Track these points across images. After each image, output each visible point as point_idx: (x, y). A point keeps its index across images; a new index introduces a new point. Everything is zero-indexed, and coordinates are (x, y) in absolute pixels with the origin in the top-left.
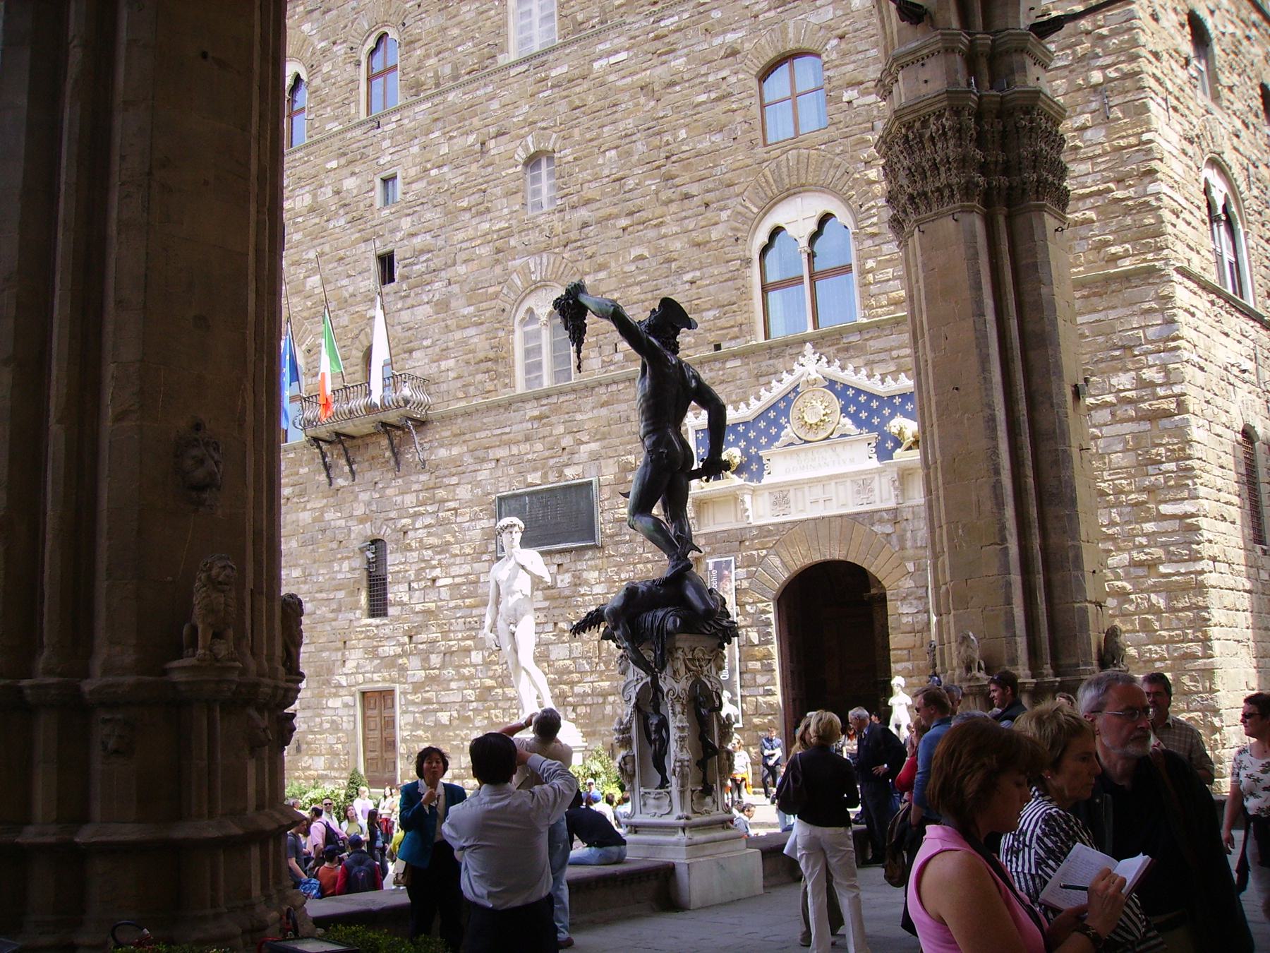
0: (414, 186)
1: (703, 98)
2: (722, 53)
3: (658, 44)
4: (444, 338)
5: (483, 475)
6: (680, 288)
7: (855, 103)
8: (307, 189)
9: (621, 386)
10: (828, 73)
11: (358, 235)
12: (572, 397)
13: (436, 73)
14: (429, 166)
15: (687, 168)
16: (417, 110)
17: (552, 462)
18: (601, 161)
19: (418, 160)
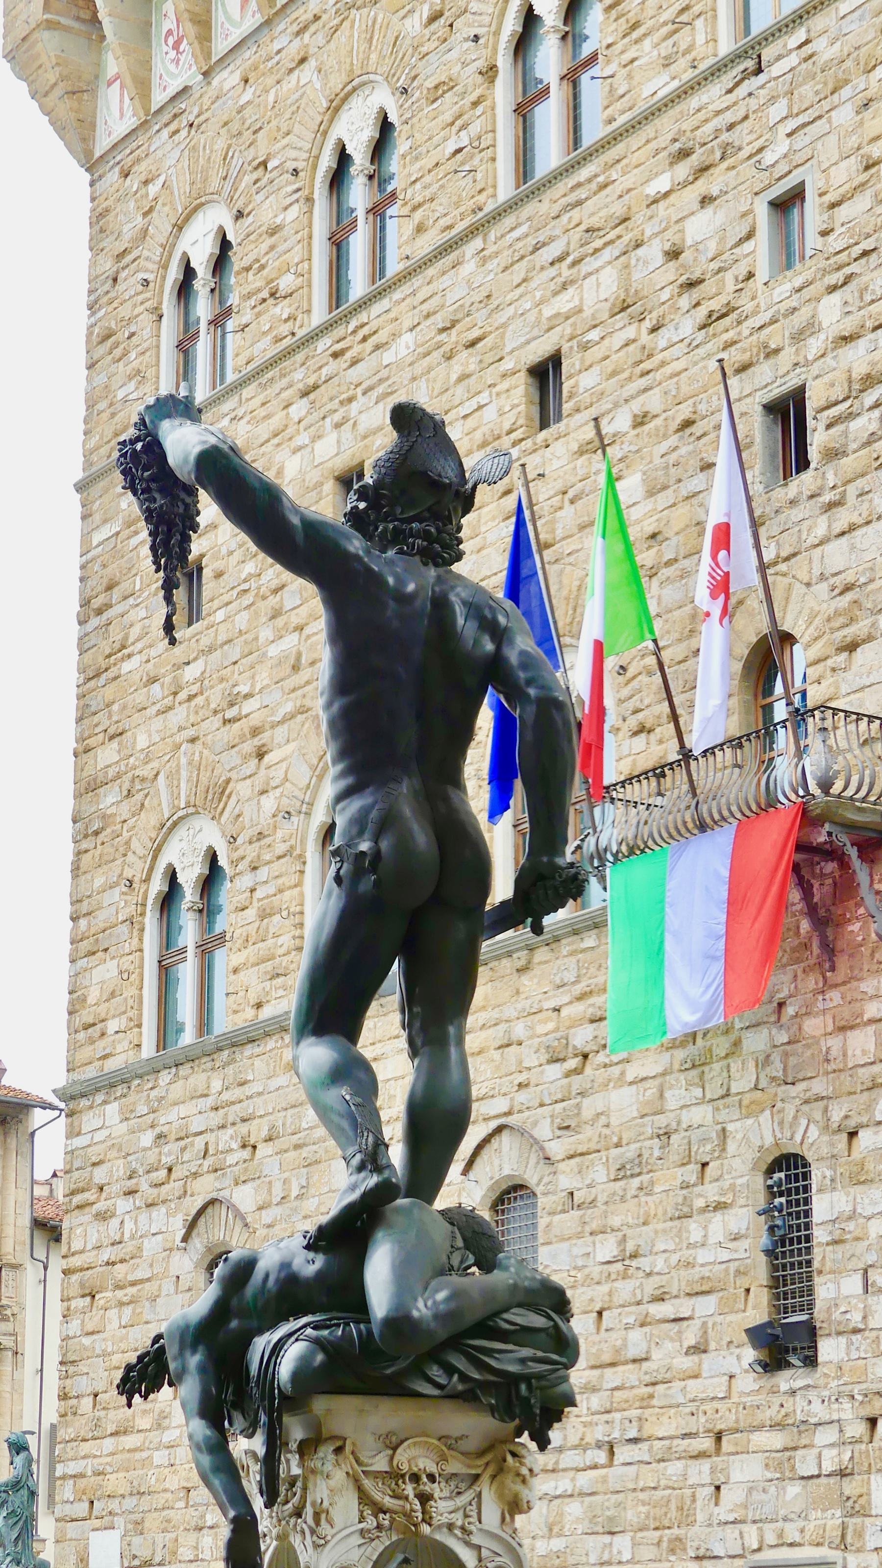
0: (843, 212)
8: (607, 254)
19: (853, 141)
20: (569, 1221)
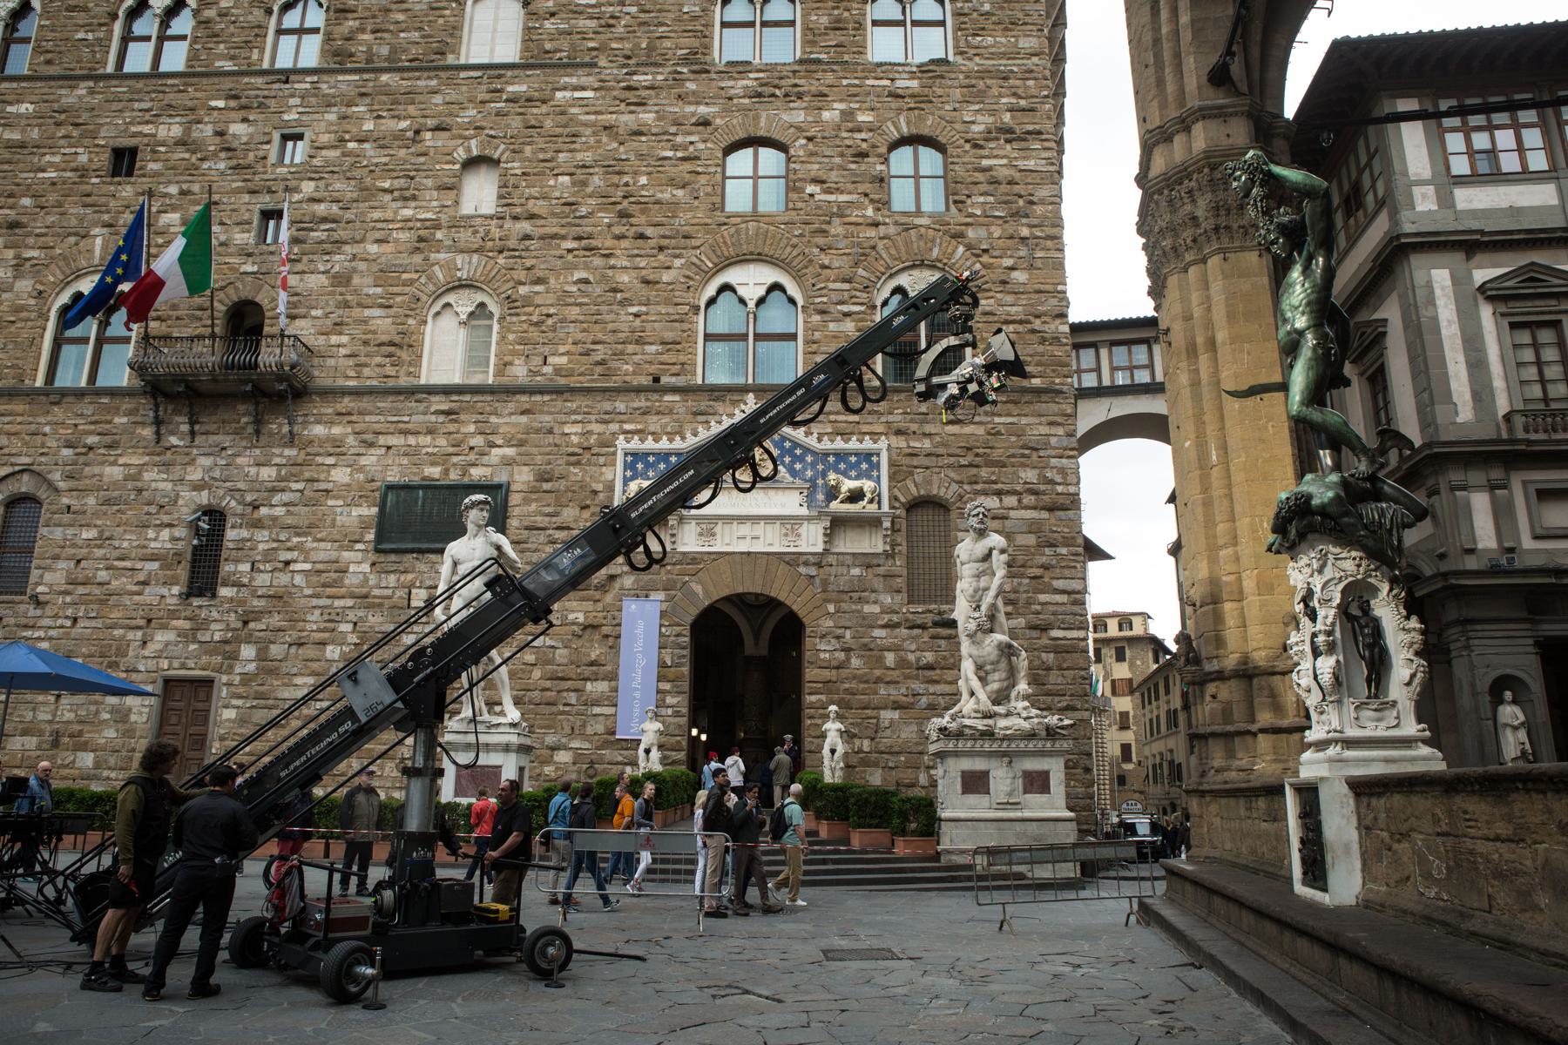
0: (324, 152)
1: (670, 154)
2: (693, 120)
3: (627, 94)
4: (341, 312)
5: (363, 461)
6: (623, 318)
7: (817, 197)
9: (546, 398)
10: (793, 166)
11: (240, 184)
12: (489, 398)
13: (370, 49)
14: (347, 137)
15: (643, 212)
16: (340, 78)
17: (455, 459)
18: (552, 182)
20: (66, 518)
